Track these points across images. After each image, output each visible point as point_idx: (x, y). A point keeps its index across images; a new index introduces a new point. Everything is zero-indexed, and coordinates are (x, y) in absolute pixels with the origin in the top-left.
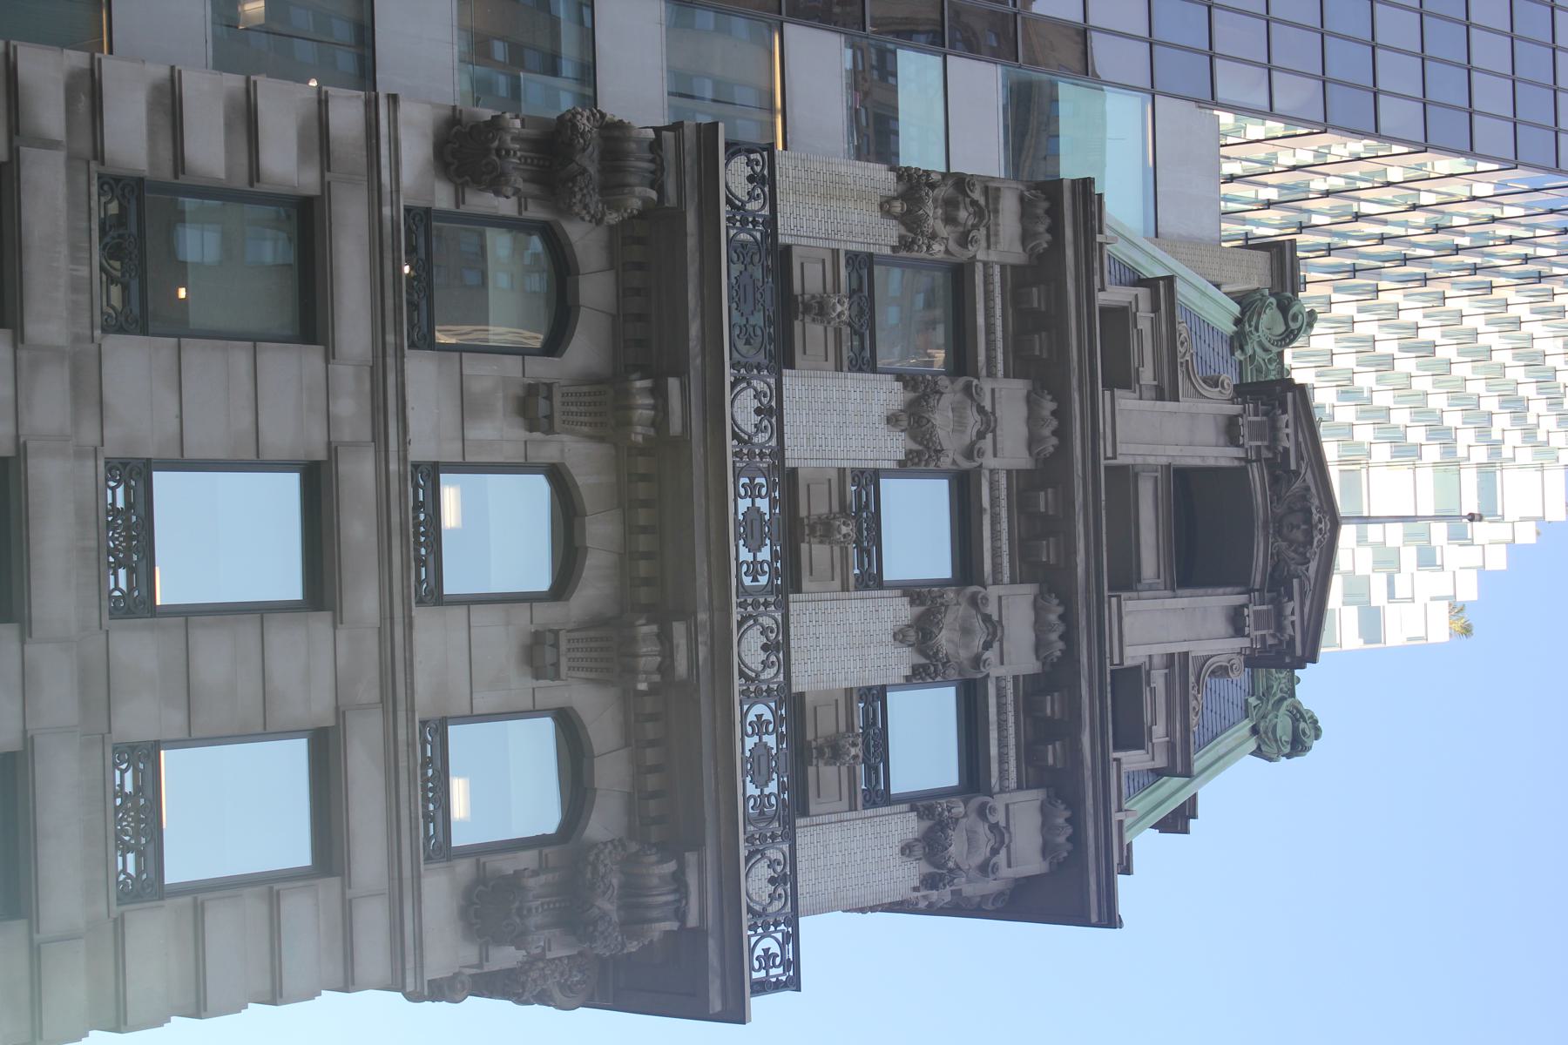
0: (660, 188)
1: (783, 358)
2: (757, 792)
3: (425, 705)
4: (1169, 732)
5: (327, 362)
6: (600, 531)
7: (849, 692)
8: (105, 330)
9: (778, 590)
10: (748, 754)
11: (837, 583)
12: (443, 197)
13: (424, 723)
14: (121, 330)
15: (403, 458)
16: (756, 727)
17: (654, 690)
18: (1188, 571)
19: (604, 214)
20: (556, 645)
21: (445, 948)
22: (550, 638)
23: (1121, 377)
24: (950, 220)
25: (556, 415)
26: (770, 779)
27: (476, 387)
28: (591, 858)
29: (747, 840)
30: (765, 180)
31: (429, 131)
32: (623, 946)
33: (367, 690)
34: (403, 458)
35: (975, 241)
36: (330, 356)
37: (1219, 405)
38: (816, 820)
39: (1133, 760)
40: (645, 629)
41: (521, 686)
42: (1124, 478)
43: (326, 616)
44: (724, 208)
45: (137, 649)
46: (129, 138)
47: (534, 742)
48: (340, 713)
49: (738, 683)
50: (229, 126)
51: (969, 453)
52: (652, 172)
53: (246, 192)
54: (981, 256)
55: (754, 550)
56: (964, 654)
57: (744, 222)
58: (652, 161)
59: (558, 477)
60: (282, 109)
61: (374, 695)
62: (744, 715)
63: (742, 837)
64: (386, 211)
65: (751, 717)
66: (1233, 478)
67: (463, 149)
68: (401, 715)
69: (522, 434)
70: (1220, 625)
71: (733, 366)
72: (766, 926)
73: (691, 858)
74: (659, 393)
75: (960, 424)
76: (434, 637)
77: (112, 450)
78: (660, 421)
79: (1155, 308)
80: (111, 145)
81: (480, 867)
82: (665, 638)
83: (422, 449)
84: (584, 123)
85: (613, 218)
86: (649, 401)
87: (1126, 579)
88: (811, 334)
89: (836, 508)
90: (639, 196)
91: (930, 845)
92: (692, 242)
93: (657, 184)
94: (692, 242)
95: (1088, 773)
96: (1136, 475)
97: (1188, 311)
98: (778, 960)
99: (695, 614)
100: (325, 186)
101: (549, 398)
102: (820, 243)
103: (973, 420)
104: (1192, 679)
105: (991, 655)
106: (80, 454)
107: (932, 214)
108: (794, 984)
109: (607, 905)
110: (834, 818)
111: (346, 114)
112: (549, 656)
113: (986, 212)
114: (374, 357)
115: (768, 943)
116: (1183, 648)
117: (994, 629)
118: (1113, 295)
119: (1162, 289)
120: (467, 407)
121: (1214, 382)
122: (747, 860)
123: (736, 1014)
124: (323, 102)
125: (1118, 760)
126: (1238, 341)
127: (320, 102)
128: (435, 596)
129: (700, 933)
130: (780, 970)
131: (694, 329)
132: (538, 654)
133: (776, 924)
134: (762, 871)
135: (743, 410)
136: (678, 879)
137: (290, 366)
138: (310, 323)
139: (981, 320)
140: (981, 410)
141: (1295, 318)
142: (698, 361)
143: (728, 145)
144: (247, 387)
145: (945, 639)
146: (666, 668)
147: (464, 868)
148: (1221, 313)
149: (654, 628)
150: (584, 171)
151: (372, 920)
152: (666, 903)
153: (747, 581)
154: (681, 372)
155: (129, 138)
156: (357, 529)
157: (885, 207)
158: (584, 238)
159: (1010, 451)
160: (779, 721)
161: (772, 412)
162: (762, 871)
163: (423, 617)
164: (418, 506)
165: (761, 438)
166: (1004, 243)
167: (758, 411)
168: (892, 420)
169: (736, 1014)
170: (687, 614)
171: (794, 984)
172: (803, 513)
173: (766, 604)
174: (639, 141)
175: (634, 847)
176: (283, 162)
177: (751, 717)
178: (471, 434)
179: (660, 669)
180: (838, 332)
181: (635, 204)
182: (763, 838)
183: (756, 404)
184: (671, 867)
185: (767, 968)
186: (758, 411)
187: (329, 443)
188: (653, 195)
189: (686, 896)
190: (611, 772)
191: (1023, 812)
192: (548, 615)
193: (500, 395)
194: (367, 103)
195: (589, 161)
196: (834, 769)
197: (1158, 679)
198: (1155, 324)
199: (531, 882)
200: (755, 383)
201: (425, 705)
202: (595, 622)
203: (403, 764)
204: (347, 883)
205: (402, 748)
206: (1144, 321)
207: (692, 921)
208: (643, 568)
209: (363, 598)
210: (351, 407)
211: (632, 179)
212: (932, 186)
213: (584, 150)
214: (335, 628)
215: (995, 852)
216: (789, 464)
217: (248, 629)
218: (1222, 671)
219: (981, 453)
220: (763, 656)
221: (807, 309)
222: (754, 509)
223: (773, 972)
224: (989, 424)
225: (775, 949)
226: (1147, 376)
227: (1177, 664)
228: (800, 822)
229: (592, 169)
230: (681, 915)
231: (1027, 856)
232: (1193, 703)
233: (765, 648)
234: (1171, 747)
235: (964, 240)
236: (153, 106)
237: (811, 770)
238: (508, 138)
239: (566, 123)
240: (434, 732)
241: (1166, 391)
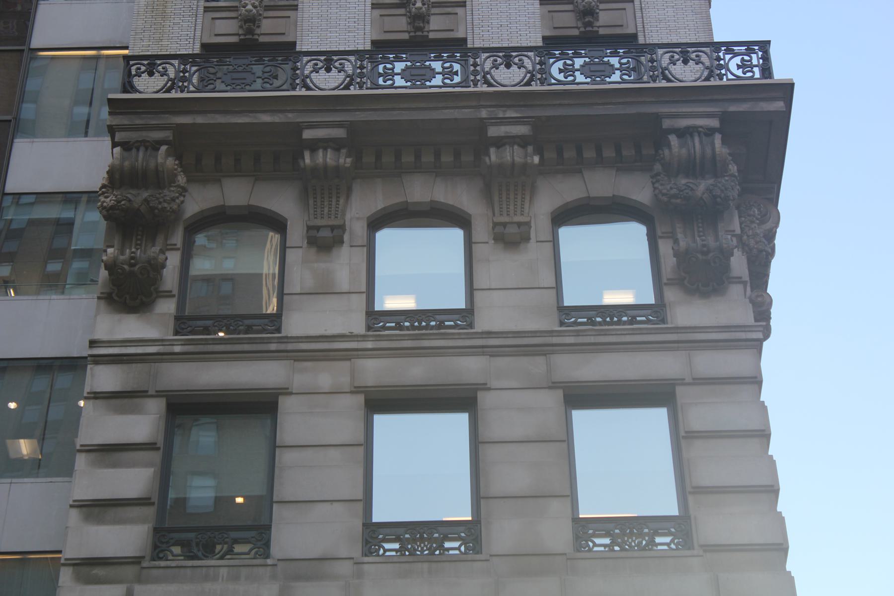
0: (159, 143)
1: (287, 51)
2: (618, 73)
3: (549, 323)
5: (291, 393)
6: (419, 190)
8: (268, 556)
9: (465, 55)
10: (589, 80)
11: (459, 10)
12: (167, 307)
13: (562, 324)
14: (267, 545)
15: (363, 338)
16: (569, 73)
17: (539, 151)
19: (179, 186)
20: (504, 225)
21: (731, 309)
22: (499, 229)
25: (330, 223)
26: (608, 63)
28: (665, 199)
29: (654, 81)
30: (152, 63)
31: (117, 317)
32: (732, 175)
33: (536, 366)
34: (363, 338)
36: (286, 392)
38: (640, 28)
40: (493, 158)
41: (535, 251)
43: (480, 395)
44: (173, 95)
45: (503, 534)
46: (125, 538)
47: (575, 240)
48: (553, 386)
49: (535, 87)
50: (115, 465)
52: (147, 149)
53: (164, 452)
55: (433, 73)
57: (184, 79)
58: (138, 150)
59: (377, 222)
60: (101, 426)
61: (541, 360)
62: (560, 82)
64: (177, 349)
65: (561, 77)
67: (130, 292)
68: (555, 340)
69: (345, 250)
71: (294, 89)
72: (720, 67)
73: (667, 123)
74: (314, 145)
76: (494, 317)
78: (336, 145)
81: (671, 283)
82: (500, 143)
83: (358, 325)
84: (109, 201)
85: (181, 179)
86: (320, 153)
88: (269, 28)
89: (402, 11)
90: (164, 159)
92: (200, 120)
93: (155, 146)
94: (200, 120)
98: (746, 58)
99: (482, 119)
100: (159, 394)
101: (318, 228)
102: (200, 21)
108: (764, 46)
109: (702, 187)
110: (638, 14)
111: (105, 378)
114: (287, 358)
115: (733, 66)
122: (669, 81)
123: (787, 90)
124: (96, 396)
127: (95, 398)
128: (467, 314)
129: (724, 118)
130: (754, 56)
131: (266, 118)
132: (511, 238)
133: (719, 59)
134: (678, 70)
135: (327, 82)
136: (683, 133)
137: (295, 422)
138: (261, 406)
142: (290, 115)
143: (125, 91)
144: (310, 452)
146: (522, 142)
147: (671, 295)
149: (492, 150)
150: (146, 201)
151: (709, 363)
152: (701, 142)
153: (457, 79)
154: (299, 128)
155: (125, 538)
156: (416, 372)
158: (197, 201)
160: (563, 56)
161: (328, 59)
162: (678, 70)
163: (482, 323)
164: (399, 327)
165: (349, 68)
167: (328, 70)
169: (787, 90)
170: (482, 125)
171: (764, 46)
172: (405, 36)
173: (475, 65)
174: (123, 159)
175: (658, 167)
176: (142, 425)
177: (561, 77)
178: (345, 287)
179: (524, 146)
181: (171, 162)
182: (653, 69)
183: (322, 71)
184: (673, 139)
185: (752, 66)
186: (328, 70)
187: (352, 392)
188: (164, 148)
190: (602, 184)
192: (481, 230)
193: (316, 265)
194: (97, 363)
195: (139, 197)
196: (601, 14)
199: (683, 244)
200: (306, 72)
201: (549, 323)
202: (487, 194)
203: (592, 339)
204: (682, 382)
205: (580, 340)
207: (715, 123)
208: (447, 158)
209: (468, 368)
210: (325, 376)
211: (152, 165)
213: (130, 201)
214: (489, 389)
216: (368, 47)
217: (490, 453)
220: (514, 68)
221: (250, 31)
222: (403, 74)
223: (755, 62)
225: (737, 60)
228: (641, 40)
229: (145, 194)
233: (508, 66)
236: (101, 521)
237: (602, 31)
238: (122, 257)
239: (109, 214)
240: (568, 315)
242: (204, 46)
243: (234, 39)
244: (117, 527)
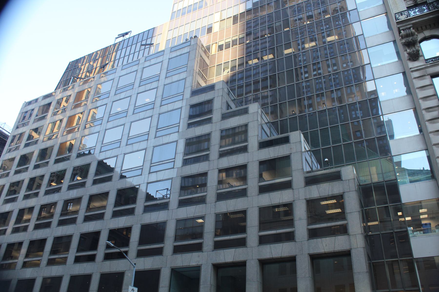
50: (425, 90)
64: (429, 65)
85: (416, 33)
90: (412, 30)
93: (410, 28)
100: (428, 75)
111: (416, 74)
124: (415, 78)
150: (412, 39)
164: (432, 61)
181: (414, 31)
188: (412, 28)
195: (410, 39)
211: (410, 32)
222: (418, 11)
229: (411, 38)
236: (426, 101)
242: (407, 8)
243: (413, 5)
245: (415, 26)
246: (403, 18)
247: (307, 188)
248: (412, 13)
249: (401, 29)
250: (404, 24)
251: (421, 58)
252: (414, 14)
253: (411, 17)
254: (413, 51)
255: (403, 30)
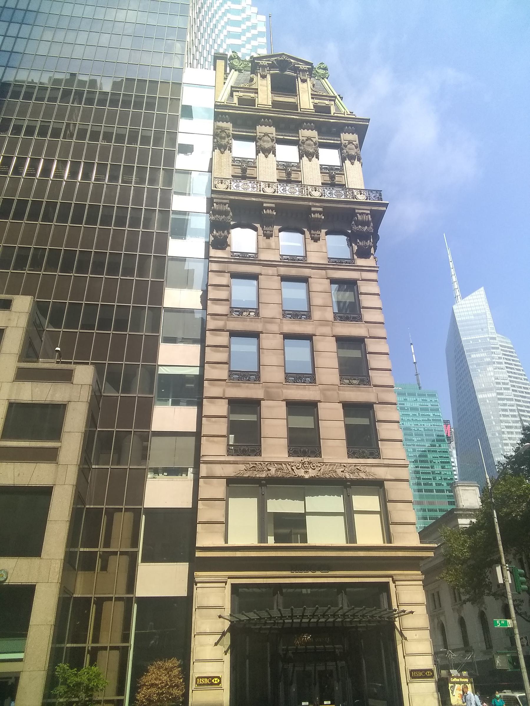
4: (327, 100)
7: (321, 173)
18: (292, 91)
20: (314, 234)
23: (252, 102)
24: (224, 138)
27: (265, 246)
35: (229, 133)
37: (257, 79)
39: (333, 110)
41: (321, 242)
42: (275, 104)
50: (218, 290)
51: (272, 140)
54: (231, 132)
56: (314, 146)
59: (280, 231)
63: (352, 200)
64: (233, 260)
66: (274, 78)
68: (328, 266)
70: (305, 85)
73: (357, 211)
75: (268, 142)
77: (281, 317)
79: (238, 91)
80: (224, 313)
87: (294, 106)
90: (227, 208)
91: (352, 158)
94: (236, 198)
95: (339, 121)
96: (273, 101)
97: (235, 83)
103: (266, 138)
104: (316, 93)
105: (314, 140)
106: (281, 323)
107: (224, 142)
112: (316, 236)
113: (223, 130)
116: (310, 95)
117: (309, 139)
118: (236, 100)
119: (233, 90)
120: (269, 248)
121: (252, 80)
125: (334, 113)
126: (240, 71)
131: (254, 199)
139: (244, 134)
140: (264, 136)
141: (235, 56)
145: (311, 151)
146: (320, 213)
148: (234, 75)
154: (262, 203)
156: (293, 272)
157: (222, 153)
159: (272, 130)
166: (228, 125)
168: (266, 157)
180: (249, 167)
181: (229, 208)
184: (358, 215)
188: (227, 205)
189: (364, 213)
191: (346, 137)
197: (316, 101)
198: (241, 92)
199: (360, 243)
205: (334, 267)
206: (241, 94)
207: (369, 212)
209: (306, 272)
210: (271, 271)
211: (224, 209)
212: (217, 141)
215: (353, 144)
218: (314, 85)
219: (273, 137)
224: (266, 134)
226: (252, 95)
227: (314, 96)
230: (367, 214)
231: (354, 137)
232: (321, 94)
234: (330, 100)
235: (228, 136)
236: (217, 305)
241: (256, 91)
243: (240, 175)
244: (221, 306)
245: (232, 204)
246: (221, 187)
247: (17, 383)
248: (234, 185)
249: (215, 200)
250: (220, 196)
251: (228, 248)
252: (235, 188)
253: (231, 190)
254: (220, 236)
255: (217, 203)
